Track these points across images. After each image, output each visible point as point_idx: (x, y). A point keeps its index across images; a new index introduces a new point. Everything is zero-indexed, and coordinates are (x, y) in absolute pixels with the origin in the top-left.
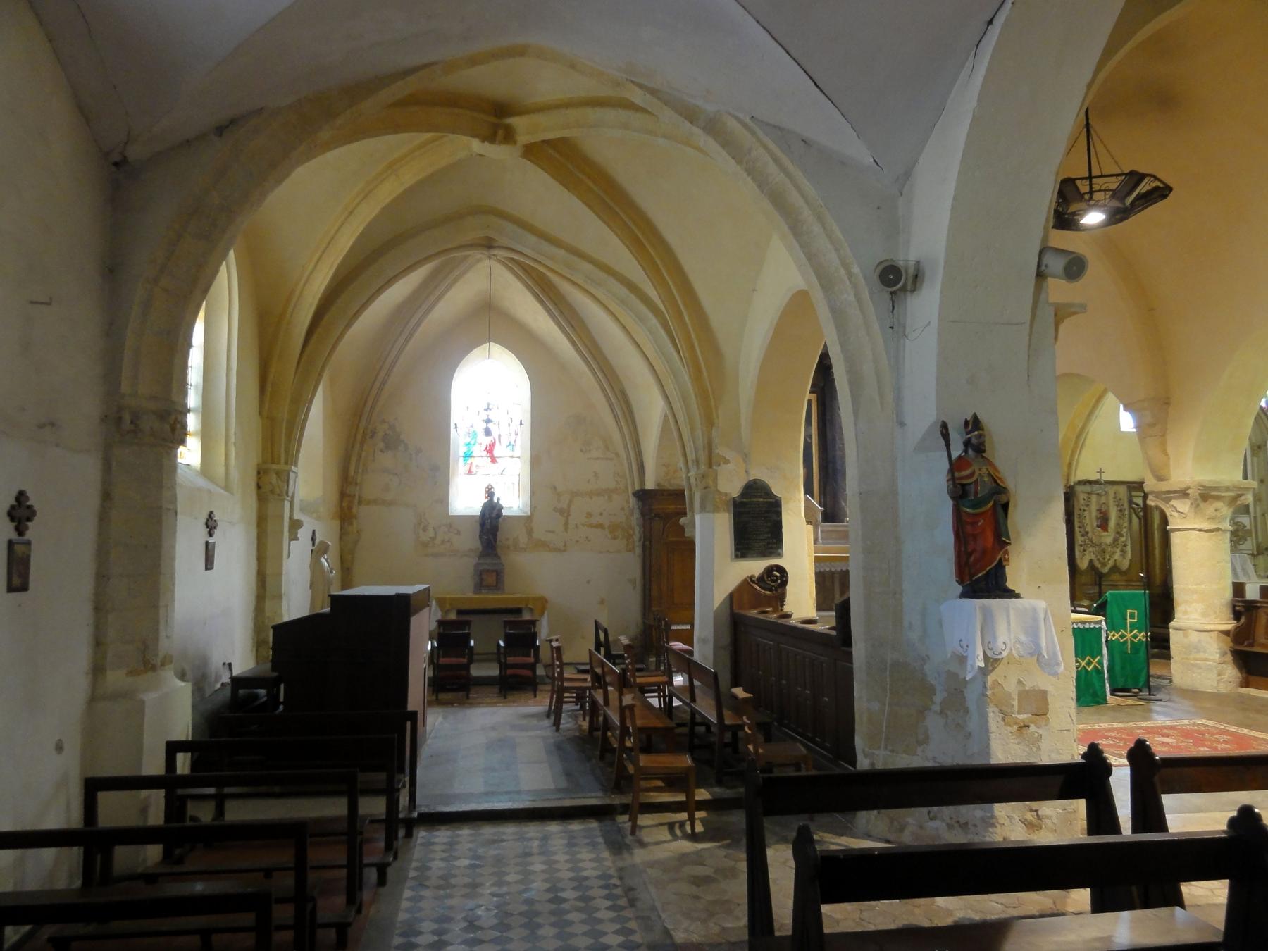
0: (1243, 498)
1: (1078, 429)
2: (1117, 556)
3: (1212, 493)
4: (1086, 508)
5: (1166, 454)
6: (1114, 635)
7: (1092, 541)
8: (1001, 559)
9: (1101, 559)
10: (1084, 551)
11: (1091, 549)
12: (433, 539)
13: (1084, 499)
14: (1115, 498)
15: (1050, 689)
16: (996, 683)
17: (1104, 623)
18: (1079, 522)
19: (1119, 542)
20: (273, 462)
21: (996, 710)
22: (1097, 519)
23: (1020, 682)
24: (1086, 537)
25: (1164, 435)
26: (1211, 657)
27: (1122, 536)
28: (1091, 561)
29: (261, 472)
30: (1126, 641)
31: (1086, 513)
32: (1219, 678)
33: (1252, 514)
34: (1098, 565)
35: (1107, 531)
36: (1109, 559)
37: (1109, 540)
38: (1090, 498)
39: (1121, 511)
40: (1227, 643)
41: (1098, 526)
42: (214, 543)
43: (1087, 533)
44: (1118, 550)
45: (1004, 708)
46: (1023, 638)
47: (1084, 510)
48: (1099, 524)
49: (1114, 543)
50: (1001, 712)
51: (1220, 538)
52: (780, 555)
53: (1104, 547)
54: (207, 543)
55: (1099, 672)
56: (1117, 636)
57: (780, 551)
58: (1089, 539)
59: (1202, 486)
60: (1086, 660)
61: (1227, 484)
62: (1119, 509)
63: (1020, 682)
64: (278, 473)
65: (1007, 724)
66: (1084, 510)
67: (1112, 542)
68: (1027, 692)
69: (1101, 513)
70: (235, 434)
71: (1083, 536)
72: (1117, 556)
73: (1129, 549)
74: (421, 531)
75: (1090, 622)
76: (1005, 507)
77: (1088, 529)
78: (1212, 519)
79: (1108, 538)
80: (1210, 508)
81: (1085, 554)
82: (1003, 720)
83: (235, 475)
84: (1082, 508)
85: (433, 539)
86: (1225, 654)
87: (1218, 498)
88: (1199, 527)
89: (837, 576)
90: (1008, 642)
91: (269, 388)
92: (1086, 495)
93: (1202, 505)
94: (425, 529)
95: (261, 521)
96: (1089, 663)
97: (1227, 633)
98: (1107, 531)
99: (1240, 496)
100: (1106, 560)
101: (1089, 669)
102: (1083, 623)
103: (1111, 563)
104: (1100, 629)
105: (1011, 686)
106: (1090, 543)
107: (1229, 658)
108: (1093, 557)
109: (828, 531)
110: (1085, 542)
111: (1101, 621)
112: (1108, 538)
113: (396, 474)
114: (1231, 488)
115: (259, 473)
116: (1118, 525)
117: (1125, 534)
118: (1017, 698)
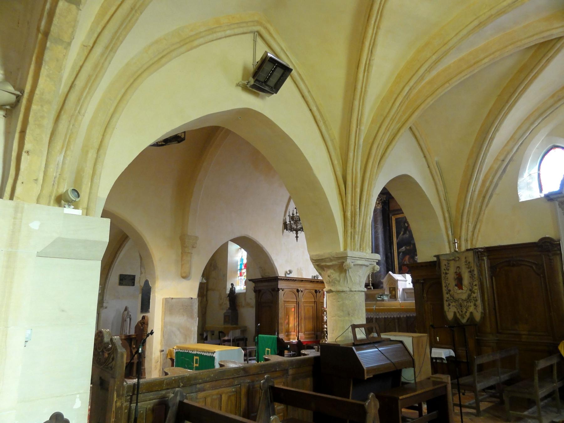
0: (344, 264)
1: (461, 211)
2: (472, 309)
3: (322, 264)
4: (447, 272)
7: (453, 298)
9: (460, 312)
10: (449, 305)
11: (454, 304)
12: (223, 303)
13: (445, 265)
14: (466, 262)
18: (445, 283)
19: (472, 297)
22: (455, 279)
24: (449, 294)
27: (474, 293)
28: (455, 313)
31: (448, 275)
34: (458, 315)
35: (462, 289)
36: (466, 312)
37: (464, 297)
38: (449, 264)
39: (470, 272)
41: (456, 286)
43: (450, 291)
44: (472, 304)
47: (446, 273)
48: (456, 283)
49: (468, 299)
51: (334, 297)
53: (460, 301)
58: (451, 296)
59: (314, 260)
62: (469, 270)
66: (446, 273)
67: (467, 298)
69: (457, 275)
71: (447, 293)
72: (472, 309)
73: (479, 302)
77: (451, 288)
79: (462, 294)
81: (450, 308)
84: (445, 272)
85: (223, 303)
87: (329, 267)
92: (447, 262)
94: (221, 299)
98: (462, 289)
99: (344, 262)
100: (464, 312)
103: (468, 314)
106: (452, 298)
108: (455, 310)
110: (449, 298)
112: (462, 294)
114: (332, 259)
116: (471, 284)
117: (476, 291)
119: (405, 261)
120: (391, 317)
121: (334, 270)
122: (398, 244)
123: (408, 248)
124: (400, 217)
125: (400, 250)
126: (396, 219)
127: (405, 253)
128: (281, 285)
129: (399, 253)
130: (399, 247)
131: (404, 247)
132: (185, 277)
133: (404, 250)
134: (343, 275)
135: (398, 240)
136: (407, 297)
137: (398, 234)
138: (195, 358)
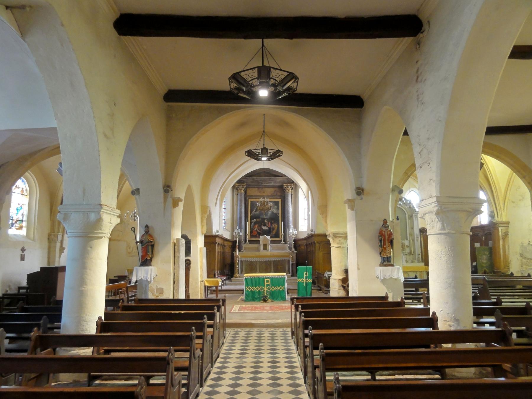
5: (326, 223)
6: (300, 280)
8: (147, 258)
12: (132, 251)
15: (164, 288)
16: (151, 287)
17: (286, 276)
20: (53, 232)
21: (151, 292)
23: (157, 286)
25: (326, 217)
26: (336, 287)
29: (49, 235)
30: (304, 282)
32: (338, 294)
33: (408, 240)
40: (341, 283)
42: (24, 255)
45: (153, 292)
46: (145, 275)
50: (152, 293)
52: (190, 256)
54: (21, 255)
55: (284, 291)
56: (301, 280)
57: (190, 255)
59: (333, 233)
60: (280, 287)
61: (342, 232)
63: (157, 286)
64: (54, 235)
65: (153, 296)
68: (159, 288)
70: (37, 226)
74: (128, 249)
75: (281, 276)
76: (153, 246)
78: (338, 243)
80: (337, 240)
82: (152, 295)
83: (37, 237)
85: (132, 251)
86: (340, 287)
87: (340, 237)
88: (334, 246)
89: (272, 263)
90: (141, 276)
91: (52, 214)
93: (335, 239)
94: (129, 248)
95: (49, 248)
96: (281, 288)
97: (340, 279)
101: (281, 290)
102: (279, 276)
104: (285, 278)
105: (154, 287)
107: (342, 288)
109: (274, 247)
111: (285, 275)
113: (121, 231)
115: (49, 235)
118: (156, 289)
119: (255, 227)
120: (269, 261)
121: (342, 238)
122: (251, 217)
123: (258, 220)
124: (254, 200)
125: (252, 221)
126: (251, 202)
127: (255, 223)
128: (218, 240)
129: (251, 223)
130: (252, 218)
131: (255, 219)
132: (202, 234)
133: (255, 221)
134: (346, 240)
135: (251, 214)
136: (272, 250)
137: (252, 211)
138: (265, 280)
